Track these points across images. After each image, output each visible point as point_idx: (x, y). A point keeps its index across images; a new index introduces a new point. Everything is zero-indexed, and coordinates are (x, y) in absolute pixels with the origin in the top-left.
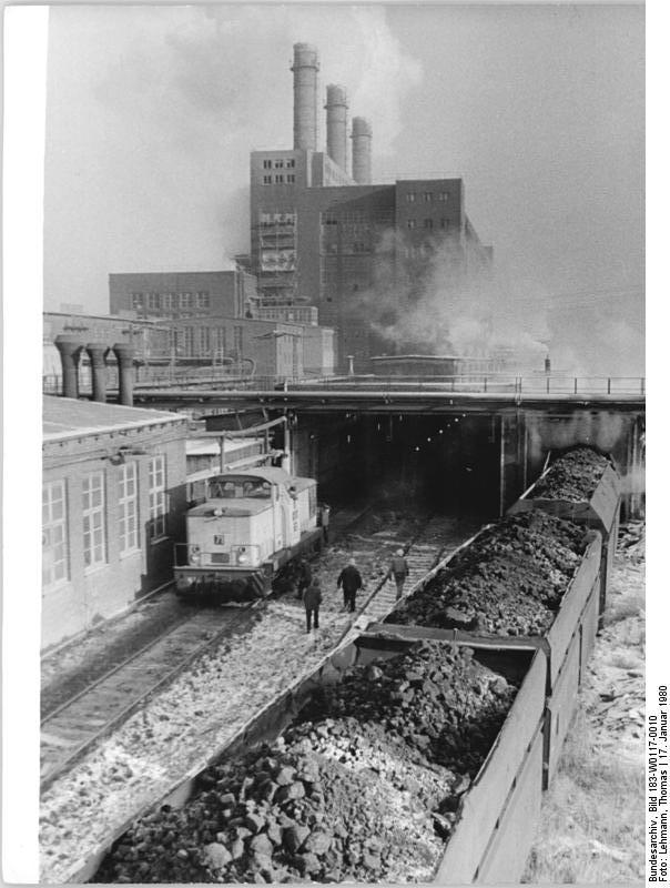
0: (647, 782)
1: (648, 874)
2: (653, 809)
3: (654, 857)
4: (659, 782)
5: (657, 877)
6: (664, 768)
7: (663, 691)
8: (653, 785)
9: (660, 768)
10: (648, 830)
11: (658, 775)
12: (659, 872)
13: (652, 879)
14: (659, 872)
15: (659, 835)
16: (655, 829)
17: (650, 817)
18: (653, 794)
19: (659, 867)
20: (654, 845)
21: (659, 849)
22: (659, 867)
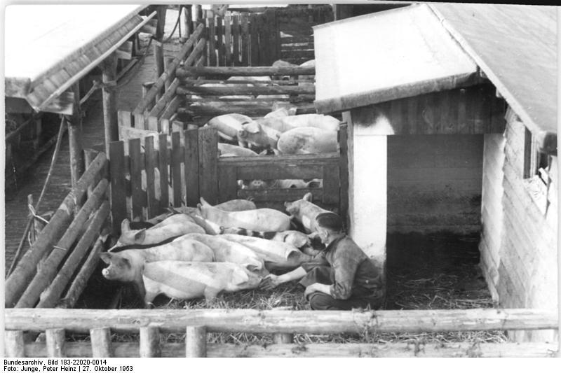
0: (67, 359)
1: (9, 360)
2: (50, 362)
3: (20, 363)
4: (67, 366)
5: (7, 365)
6: (77, 369)
7: (124, 368)
8: (65, 363)
9: (77, 366)
10: (36, 359)
11: (71, 365)
12: (10, 366)
13: (5, 362)
14: (10, 366)
15: (35, 366)
16: (38, 363)
17: (45, 361)
18: (59, 362)
19: (14, 366)
20: (27, 363)
21: (26, 366)
22: (14, 366)
